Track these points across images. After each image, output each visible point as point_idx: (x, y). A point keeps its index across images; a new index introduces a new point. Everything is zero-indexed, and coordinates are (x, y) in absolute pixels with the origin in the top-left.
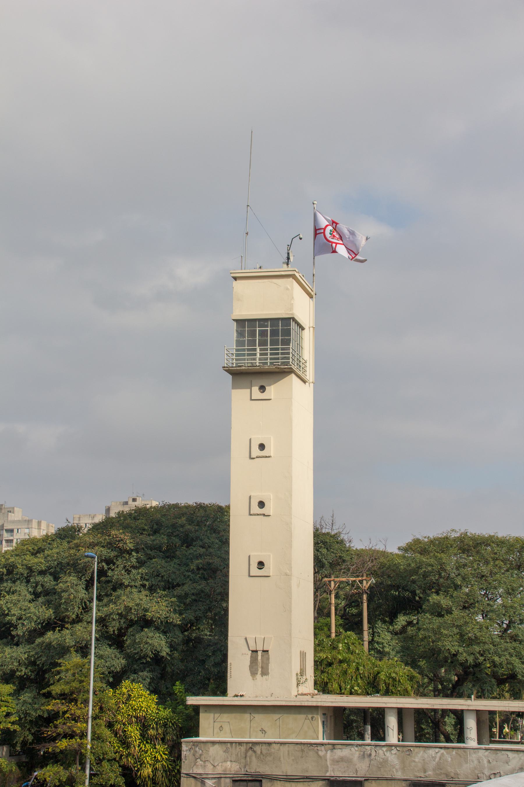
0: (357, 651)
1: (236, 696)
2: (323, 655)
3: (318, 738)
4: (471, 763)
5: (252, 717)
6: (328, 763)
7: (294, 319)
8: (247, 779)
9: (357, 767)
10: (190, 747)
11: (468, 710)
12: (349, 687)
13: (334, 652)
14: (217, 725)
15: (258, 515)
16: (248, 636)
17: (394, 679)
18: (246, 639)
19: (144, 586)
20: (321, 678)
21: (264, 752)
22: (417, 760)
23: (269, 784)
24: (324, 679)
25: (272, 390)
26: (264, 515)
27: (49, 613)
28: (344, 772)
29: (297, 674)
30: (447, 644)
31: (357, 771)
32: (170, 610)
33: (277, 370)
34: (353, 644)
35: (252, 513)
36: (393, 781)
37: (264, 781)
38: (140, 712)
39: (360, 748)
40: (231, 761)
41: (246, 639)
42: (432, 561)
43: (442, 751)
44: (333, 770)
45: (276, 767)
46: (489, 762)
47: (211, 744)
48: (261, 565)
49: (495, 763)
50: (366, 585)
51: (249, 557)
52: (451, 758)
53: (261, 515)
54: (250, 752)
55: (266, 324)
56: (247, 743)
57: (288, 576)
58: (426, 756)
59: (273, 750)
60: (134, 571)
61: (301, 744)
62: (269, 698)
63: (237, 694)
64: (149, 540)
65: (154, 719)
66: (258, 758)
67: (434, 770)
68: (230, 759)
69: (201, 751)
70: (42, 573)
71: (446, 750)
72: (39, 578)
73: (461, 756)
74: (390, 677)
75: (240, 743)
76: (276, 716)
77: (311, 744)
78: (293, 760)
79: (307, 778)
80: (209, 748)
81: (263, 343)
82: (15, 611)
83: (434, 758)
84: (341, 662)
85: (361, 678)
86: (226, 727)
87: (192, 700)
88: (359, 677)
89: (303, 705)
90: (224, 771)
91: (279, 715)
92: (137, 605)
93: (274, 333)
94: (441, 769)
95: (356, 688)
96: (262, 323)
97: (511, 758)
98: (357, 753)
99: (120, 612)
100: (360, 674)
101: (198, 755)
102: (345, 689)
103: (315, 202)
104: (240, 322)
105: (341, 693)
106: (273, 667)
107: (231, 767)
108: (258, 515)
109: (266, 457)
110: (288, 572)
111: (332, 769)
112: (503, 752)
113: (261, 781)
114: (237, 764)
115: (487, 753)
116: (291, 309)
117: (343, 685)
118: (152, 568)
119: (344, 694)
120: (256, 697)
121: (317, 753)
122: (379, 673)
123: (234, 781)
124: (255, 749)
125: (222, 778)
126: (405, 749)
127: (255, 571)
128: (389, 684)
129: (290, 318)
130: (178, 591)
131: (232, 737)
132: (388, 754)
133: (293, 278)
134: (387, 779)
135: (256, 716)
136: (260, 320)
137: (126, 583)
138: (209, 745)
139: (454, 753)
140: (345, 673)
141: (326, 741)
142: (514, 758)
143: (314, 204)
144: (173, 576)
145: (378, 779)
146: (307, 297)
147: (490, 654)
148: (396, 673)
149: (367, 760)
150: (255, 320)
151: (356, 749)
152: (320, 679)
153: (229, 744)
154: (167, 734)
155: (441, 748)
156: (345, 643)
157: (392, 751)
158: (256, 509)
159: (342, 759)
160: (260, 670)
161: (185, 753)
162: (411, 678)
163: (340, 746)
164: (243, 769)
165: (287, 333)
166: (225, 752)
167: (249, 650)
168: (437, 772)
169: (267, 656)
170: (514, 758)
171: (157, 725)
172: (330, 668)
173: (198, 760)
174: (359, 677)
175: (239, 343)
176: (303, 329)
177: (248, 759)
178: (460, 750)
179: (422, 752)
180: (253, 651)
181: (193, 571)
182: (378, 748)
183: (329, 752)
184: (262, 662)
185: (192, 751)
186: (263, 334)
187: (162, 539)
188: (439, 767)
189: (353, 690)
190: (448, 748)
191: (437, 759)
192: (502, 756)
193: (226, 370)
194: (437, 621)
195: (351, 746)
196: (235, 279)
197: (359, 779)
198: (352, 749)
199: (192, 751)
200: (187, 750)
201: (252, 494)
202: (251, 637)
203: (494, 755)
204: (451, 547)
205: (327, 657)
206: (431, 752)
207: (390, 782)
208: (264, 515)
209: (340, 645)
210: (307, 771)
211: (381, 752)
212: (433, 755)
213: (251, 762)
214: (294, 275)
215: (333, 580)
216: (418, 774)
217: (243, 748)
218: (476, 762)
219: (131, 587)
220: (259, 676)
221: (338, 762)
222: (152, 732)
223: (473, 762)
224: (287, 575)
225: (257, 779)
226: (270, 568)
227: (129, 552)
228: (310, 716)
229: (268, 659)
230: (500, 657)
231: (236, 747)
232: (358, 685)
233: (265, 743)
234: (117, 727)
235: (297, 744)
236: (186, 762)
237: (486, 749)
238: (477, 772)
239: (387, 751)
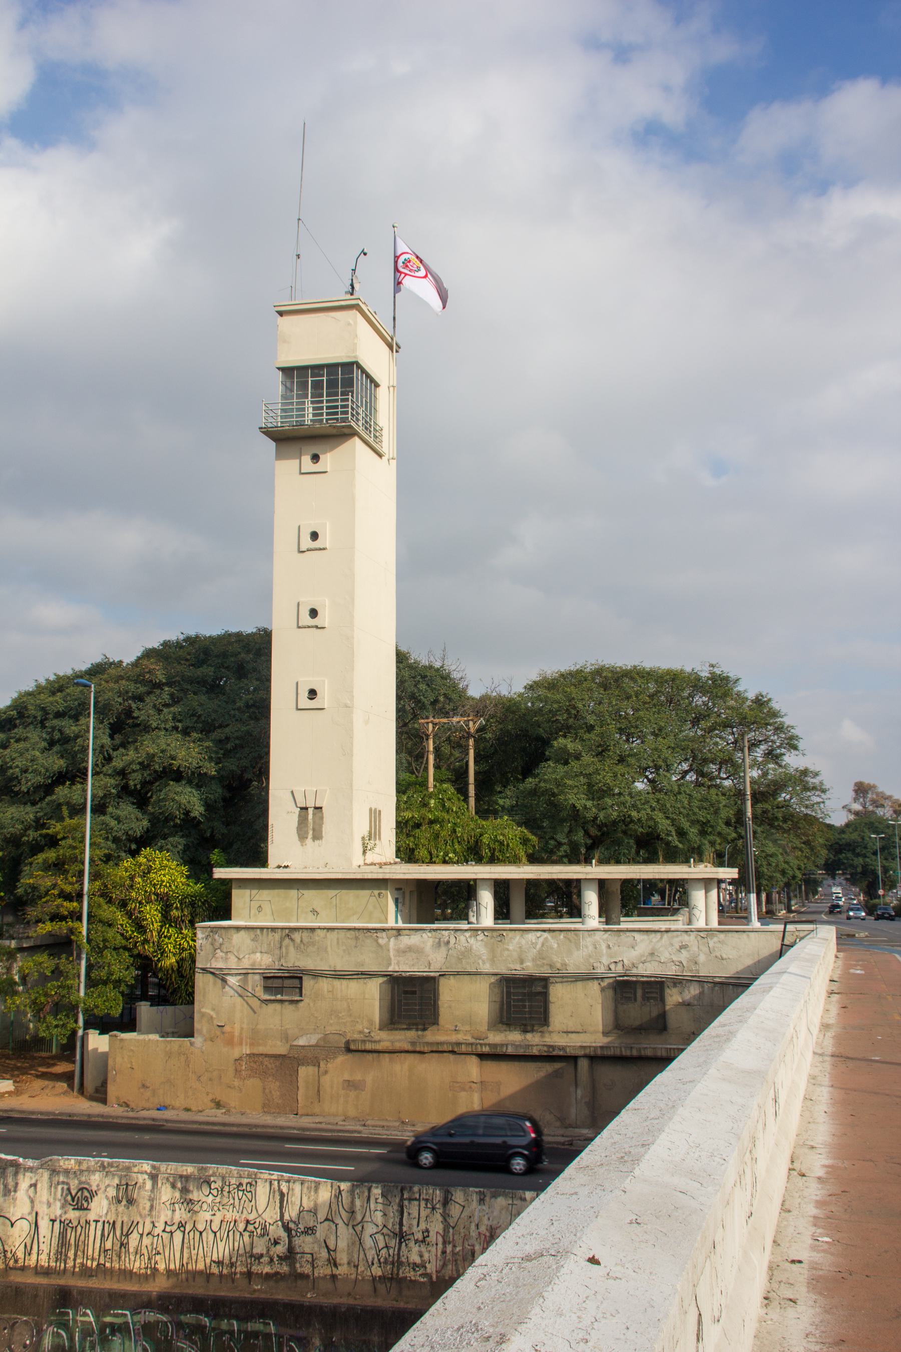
0: (454, 809)
1: (279, 867)
2: (408, 814)
3: (386, 921)
4: (585, 949)
5: (300, 895)
6: (392, 954)
7: (359, 366)
8: (283, 975)
9: (430, 958)
10: (207, 934)
11: (586, 879)
12: (442, 853)
13: (424, 811)
14: (255, 905)
15: (309, 627)
16: (295, 789)
18: (292, 792)
19: (175, 728)
20: (405, 843)
21: (305, 940)
22: (511, 948)
23: (312, 982)
24: (409, 845)
25: (328, 459)
26: (317, 627)
27: (59, 764)
28: (413, 965)
29: (363, 838)
30: (570, 797)
31: (430, 964)
32: (204, 758)
33: (334, 431)
34: (449, 799)
35: (300, 625)
36: (478, 976)
37: (305, 978)
38: (160, 888)
39: (434, 933)
40: (261, 952)
41: (292, 792)
42: (558, 697)
43: (546, 935)
44: (398, 963)
45: (321, 960)
46: (609, 947)
47: (235, 931)
48: (313, 693)
49: (616, 948)
50: (473, 727)
51: (297, 683)
52: (558, 944)
53: (312, 627)
54: (287, 941)
55: (322, 372)
56: (283, 929)
57: (349, 707)
58: (523, 942)
59: (317, 938)
60: (165, 710)
61: (355, 929)
62: (321, 870)
63: (280, 864)
64: (190, 672)
65: (178, 897)
66: (297, 948)
67: (534, 960)
68: (259, 949)
69: (221, 939)
70: (59, 715)
71: (552, 934)
72: (56, 722)
73: (570, 941)
74: (496, 840)
75: (273, 929)
76: (332, 893)
77: (368, 930)
78: (344, 951)
79: (363, 973)
80: (232, 936)
82: (20, 762)
83: (534, 945)
84: (431, 822)
85: (459, 842)
86: (267, 908)
87: (220, 873)
88: (455, 841)
89: (366, 877)
90: (252, 965)
91: (336, 892)
92: (163, 751)
93: (332, 384)
94: (543, 959)
95: (451, 855)
96: (316, 371)
97: (638, 940)
98: (431, 940)
99: (140, 760)
100: (457, 837)
101: (217, 945)
102: (437, 857)
103: (395, 225)
104: (287, 371)
105: (431, 862)
107: (262, 960)
108: (309, 627)
109: (320, 549)
110: (349, 702)
111: (396, 962)
112: (628, 934)
113: (301, 978)
114: (269, 956)
115: (606, 935)
116: (354, 350)
117: (434, 852)
118: (188, 706)
119: (435, 863)
120: (306, 868)
121: (377, 941)
122: (481, 835)
123: (265, 978)
124: (293, 936)
125: (250, 975)
126: (495, 934)
127: (304, 702)
128: (494, 849)
129: (351, 364)
130: (217, 734)
131: (274, 920)
132: (472, 941)
133: (357, 310)
134: (469, 974)
135: (306, 892)
137: (154, 725)
138: (233, 931)
139: (562, 937)
140: (437, 836)
141: (400, 924)
142: (642, 941)
143: (394, 227)
144: (214, 716)
145: (458, 974)
146: (387, 349)
147: (626, 807)
148: (504, 835)
149: (443, 950)
150: (305, 368)
151: (429, 934)
152: (404, 845)
153: (258, 930)
154: (196, 915)
155: (544, 931)
156: (440, 799)
157: (478, 937)
158: (306, 619)
159: (410, 949)
160: (311, 833)
161: (200, 942)
162: (525, 841)
163: (407, 932)
164: (277, 963)
165: (349, 383)
166: (253, 940)
167: (297, 807)
168: (538, 962)
169: (320, 815)
170: (642, 941)
171: (181, 904)
172: (418, 831)
173: (218, 951)
174: (455, 841)
176: (377, 385)
177: (284, 949)
178: (569, 933)
179: (518, 937)
180: (302, 808)
181: (239, 709)
182: (459, 933)
183: (392, 940)
184: (314, 822)
185: (210, 940)
186: (317, 385)
187: (207, 671)
188: (541, 955)
189: (447, 858)
190: (554, 931)
191: (539, 946)
192: (626, 938)
193: (263, 432)
194: (561, 769)
195: (422, 932)
196: (281, 314)
197: (432, 974)
198: (424, 935)
199: (210, 940)
200: (203, 938)
201: (302, 600)
202: (299, 790)
203: (616, 938)
204: (586, 680)
205: (413, 817)
206: (531, 936)
207: (474, 977)
208: (317, 627)
209: (432, 801)
210: (363, 965)
211: (462, 938)
212: (534, 941)
213: (287, 953)
214: (358, 305)
215: (432, 722)
216: (512, 966)
217: (277, 936)
218: (591, 948)
219: (159, 729)
220: (309, 840)
221: (404, 952)
222: (175, 913)
223: (587, 947)
224: (347, 707)
225: (296, 975)
226: (325, 698)
227: (159, 686)
228: (376, 892)
229: (322, 818)
230: (638, 812)
231: (268, 934)
232: (455, 852)
233: (307, 929)
234: (131, 906)
235: (350, 929)
236: (202, 953)
238: (592, 961)
239: (470, 937)
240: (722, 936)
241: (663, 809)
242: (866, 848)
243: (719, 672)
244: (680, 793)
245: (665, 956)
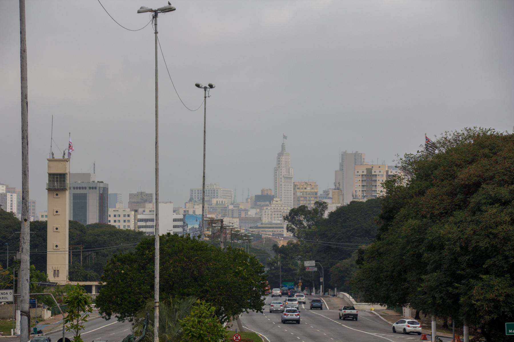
17: (92, 276)
48: (57, 246)
81: (57, 181)
93: (60, 178)
106: (60, 274)
175: (49, 181)
180: (54, 270)
186: (57, 178)
202: (54, 266)
220: (56, 277)
229: (59, 272)
243: (140, 231)
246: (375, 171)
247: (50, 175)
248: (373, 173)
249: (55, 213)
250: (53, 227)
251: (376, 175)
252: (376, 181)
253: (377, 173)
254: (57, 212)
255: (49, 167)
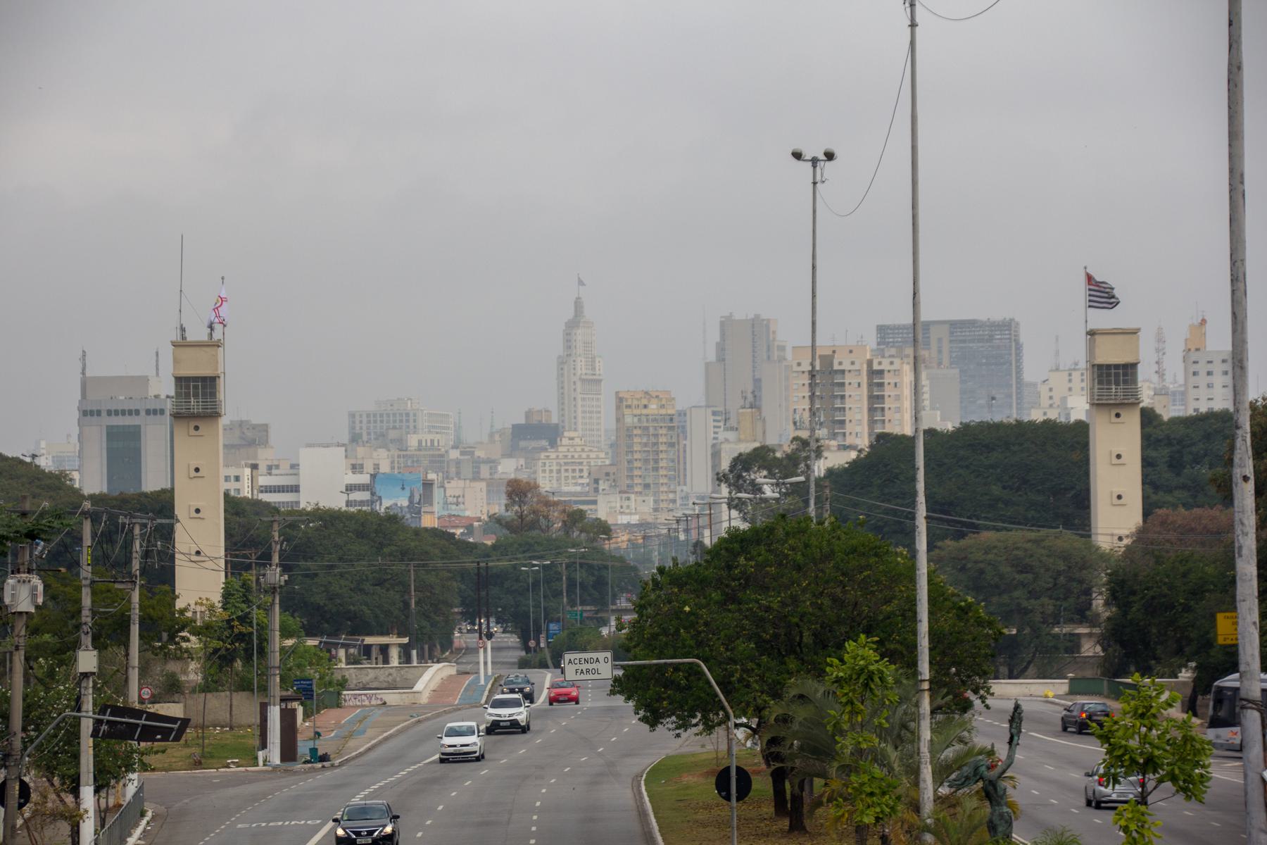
81: (196, 396)
136: (193, 377)
186: (196, 387)
192: (364, 672)
237: (355, 668)
240: (407, 669)
241: (366, 604)
242: (517, 580)
243: (391, 513)
244: (373, 594)
245: (382, 679)
246: (842, 361)
247: (179, 380)
248: (836, 367)
249: (193, 474)
250: (190, 506)
251: (843, 372)
252: (843, 384)
253: (846, 366)
254: (197, 470)
255: (176, 361)
